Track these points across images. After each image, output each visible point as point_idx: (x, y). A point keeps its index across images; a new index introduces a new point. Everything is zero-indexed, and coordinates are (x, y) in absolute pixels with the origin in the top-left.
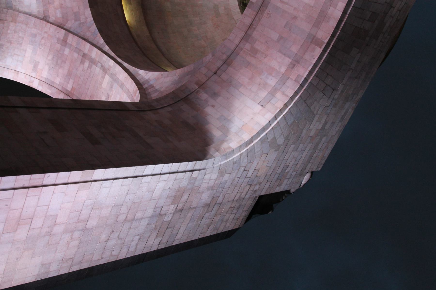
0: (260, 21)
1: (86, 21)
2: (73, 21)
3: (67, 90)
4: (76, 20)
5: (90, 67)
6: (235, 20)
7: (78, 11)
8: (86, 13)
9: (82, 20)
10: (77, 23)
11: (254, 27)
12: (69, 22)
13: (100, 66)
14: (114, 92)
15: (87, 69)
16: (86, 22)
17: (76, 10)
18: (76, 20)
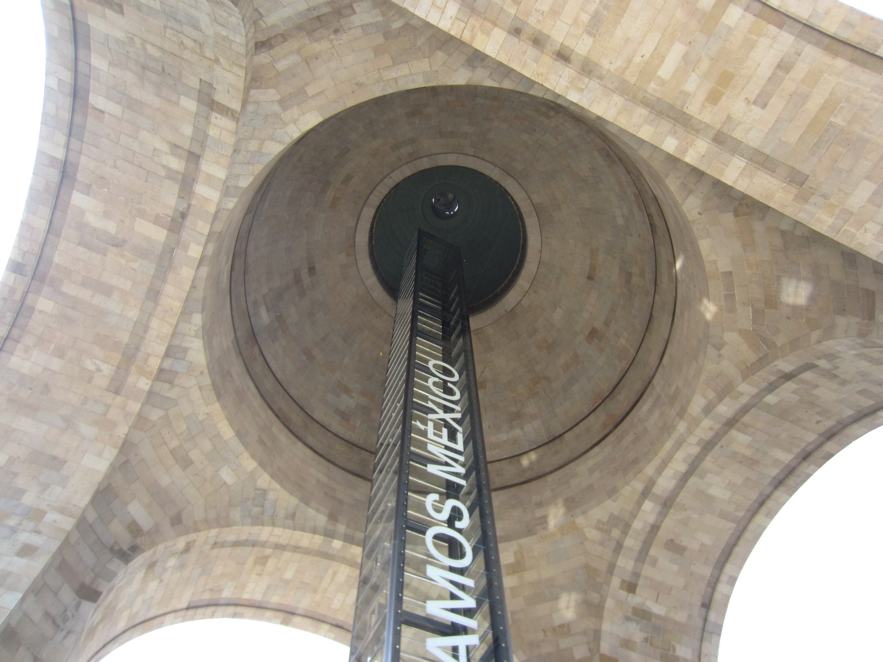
0: (307, 554)
1: (287, 124)
2: (278, 97)
3: (87, 92)
4: (281, 102)
5: (171, 174)
6: (391, 175)
7: (310, 96)
8: (308, 115)
9: (287, 116)
10: (277, 108)
11: (298, 550)
12: (272, 91)
13: (181, 209)
14: (136, 265)
15: (164, 167)
16: (285, 124)
17: (311, 90)
18: (281, 102)
